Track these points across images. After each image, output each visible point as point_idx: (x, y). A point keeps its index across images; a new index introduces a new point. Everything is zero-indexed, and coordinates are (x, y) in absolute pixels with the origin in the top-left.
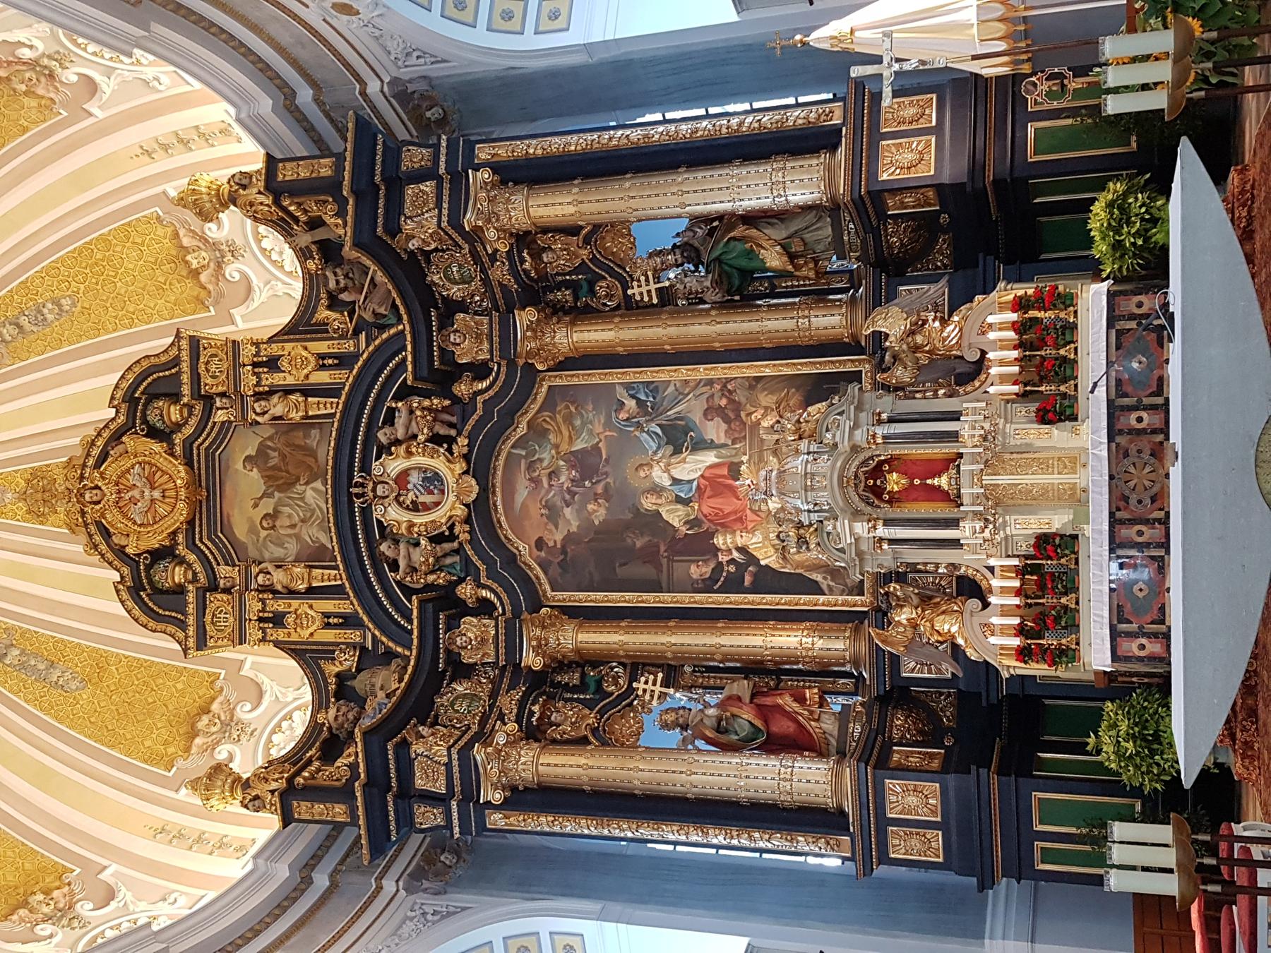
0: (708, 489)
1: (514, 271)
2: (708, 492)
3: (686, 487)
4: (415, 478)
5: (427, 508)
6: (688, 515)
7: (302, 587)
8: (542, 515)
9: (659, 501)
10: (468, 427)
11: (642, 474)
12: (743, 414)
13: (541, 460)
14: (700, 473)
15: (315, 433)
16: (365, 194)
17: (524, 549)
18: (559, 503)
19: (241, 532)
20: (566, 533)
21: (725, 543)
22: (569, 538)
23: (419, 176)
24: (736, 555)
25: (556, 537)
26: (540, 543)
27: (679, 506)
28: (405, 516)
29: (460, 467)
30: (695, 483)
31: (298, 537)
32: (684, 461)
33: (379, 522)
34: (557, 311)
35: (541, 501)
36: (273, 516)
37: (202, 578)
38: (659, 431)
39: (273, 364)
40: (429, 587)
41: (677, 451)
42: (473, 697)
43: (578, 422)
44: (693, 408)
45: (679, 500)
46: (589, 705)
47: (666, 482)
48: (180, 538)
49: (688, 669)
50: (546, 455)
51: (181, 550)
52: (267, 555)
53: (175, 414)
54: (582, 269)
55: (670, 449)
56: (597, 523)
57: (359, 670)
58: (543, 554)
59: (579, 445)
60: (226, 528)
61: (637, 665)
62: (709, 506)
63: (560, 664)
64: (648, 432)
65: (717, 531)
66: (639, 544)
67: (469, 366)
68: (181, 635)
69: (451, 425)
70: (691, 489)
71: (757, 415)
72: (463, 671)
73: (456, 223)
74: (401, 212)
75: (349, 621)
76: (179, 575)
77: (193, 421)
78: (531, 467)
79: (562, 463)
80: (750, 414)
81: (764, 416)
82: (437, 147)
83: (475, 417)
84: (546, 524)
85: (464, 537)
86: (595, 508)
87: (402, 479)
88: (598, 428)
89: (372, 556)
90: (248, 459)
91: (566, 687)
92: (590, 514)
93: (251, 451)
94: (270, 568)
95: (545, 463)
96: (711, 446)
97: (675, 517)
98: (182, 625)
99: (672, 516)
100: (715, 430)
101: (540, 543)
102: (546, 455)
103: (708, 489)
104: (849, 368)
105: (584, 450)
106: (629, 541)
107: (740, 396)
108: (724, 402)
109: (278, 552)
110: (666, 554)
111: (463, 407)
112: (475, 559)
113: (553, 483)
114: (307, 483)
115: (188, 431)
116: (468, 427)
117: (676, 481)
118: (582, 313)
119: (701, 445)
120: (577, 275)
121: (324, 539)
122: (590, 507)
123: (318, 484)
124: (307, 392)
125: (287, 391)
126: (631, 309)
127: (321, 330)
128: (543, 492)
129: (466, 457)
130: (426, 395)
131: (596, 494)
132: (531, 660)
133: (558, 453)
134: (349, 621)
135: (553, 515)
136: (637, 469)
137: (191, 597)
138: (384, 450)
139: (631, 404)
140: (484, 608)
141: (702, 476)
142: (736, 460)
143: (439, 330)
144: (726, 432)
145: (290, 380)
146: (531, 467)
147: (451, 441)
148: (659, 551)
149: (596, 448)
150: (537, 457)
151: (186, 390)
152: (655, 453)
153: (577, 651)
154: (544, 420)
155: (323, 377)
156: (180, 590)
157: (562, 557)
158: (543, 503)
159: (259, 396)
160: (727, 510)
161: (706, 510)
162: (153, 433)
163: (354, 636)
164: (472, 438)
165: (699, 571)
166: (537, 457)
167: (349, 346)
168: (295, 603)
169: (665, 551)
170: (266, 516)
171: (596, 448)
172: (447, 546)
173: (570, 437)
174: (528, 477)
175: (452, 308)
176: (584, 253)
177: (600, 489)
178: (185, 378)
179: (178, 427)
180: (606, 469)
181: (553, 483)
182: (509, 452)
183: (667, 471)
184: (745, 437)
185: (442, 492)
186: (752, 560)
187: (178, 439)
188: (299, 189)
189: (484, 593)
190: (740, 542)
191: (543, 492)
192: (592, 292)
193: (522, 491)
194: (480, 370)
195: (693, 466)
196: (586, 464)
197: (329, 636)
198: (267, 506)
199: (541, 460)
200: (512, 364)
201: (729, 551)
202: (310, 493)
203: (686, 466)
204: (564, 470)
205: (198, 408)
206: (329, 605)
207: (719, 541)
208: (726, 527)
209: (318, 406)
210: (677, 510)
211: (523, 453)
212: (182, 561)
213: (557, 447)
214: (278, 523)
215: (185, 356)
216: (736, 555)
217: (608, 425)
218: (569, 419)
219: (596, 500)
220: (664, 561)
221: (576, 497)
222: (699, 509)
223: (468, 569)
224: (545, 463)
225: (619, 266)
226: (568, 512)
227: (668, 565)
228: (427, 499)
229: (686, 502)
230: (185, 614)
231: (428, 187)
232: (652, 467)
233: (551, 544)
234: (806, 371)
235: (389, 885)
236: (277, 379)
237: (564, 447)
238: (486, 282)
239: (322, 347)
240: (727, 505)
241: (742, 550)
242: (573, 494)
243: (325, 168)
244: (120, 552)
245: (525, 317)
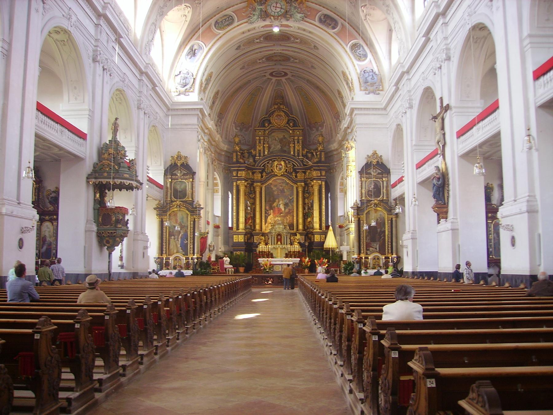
1: (309, 183)
4: (281, 166)
5: (276, 168)
7: (265, 145)
10: (288, 174)
15: (288, 147)
16: (318, 166)
17: (270, 182)
19: (273, 134)
22: (272, 188)
23: (321, 173)
24: (270, 213)
25: (272, 187)
28: (275, 165)
29: (282, 173)
31: (272, 144)
33: (274, 161)
34: (304, 188)
36: (276, 140)
37: (266, 129)
39: (298, 142)
40: (265, 168)
41: (284, 205)
42: (249, 176)
43: (289, 190)
44: (290, 207)
45: (277, 205)
46: (248, 193)
47: (280, 203)
48: (272, 125)
49: (254, 206)
50: (284, 185)
51: (270, 125)
52: (270, 138)
53: (291, 124)
54: (310, 192)
57: (252, 156)
59: (285, 190)
60: (274, 132)
61: (254, 199)
62: (276, 210)
63: (254, 188)
66: (272, 199)
67: (297, 175)
68: (257, 126)
69: (288, 172)
71: (289, 216)
72: (253, 173)
73: (314, 179)
74: (316, 171)
75: (260, 154)
76: (266, 125)
77: (290, 128)
82: (325, 176)
83: (289, 175)
85: (272, 174)
87: (281, 165)
88: (288, 193)
89: (269, 159)
90: (284, 136)
91: (251, 188)
93: (286, 136)
94: (268, 140)
96: (285, 210)
97: (275, 204)
98: (258, 127)
100: (287, 210)
101: (271, 184)
102: (284, 185)
104: (295, 229)
107: (291, 214)
108: (291, 212)
109: (270, 141)
111: (291, 174)
112: (269, 175)
114: (281, 146)
115: (289, 126)
116: (288, 174)
117: (280, 204)
118: (304, 192)
119: (285, 208)
121: (272, 148)
122: (277, 192)
123: (280, 148)
124: (294, 147)
125: (294, 144)
126: (304, 199)
127: (303, 150)
129: (284, 174)
130: (293, 168)
132: (255, 184)
134: (260, 154)
135: (275, 186)
137: (263, 128)
138: (285, 163)
139: (291, 198)
140: (262, 177)
143: (302, 171)
145: (296, 145)
146: (282, 183)
147: (286, 172)
149: (285, 193)
151: (295, 128)
153: (256, 191)
155: (296, 150)
156: (264, 126)
159: (294, 139)
162: (288, 120)
163: (258, 155)
164: (287, 175)
165: (267, 207)
167: (301, 154)
168: (262, 145)
170: (275, 139)
171: (285, 193)
172: (271, 171)
175: (305, 173)
176: (311, 193)
177: (279, 193)
178: (297, 128)
179: (289, 125)
185: (279, 171)
186: (269, 215)
187: (288, 125)
188: (320, 155)
189: (264, 177)
190: (272, 214)
192: (307, 193)
193: (279, 181)
194: (296, 176)
195: (282, 207)
196: (283, 191)
197: (257, 150)
198: (277, 139)
200: (297, 181)
202: (279, 146)
205: (292, 129)
206: (262, 150)
207: (272, 211)
208: (273, 212)
209: (292, 149)
212: (269, 125)
213: (285, 187)
214: (274, 141)
215: (300, 128)
216: (270, 213)
217: (288, 195)
218: (289, 188)
223: (267, 174)
226: (276, 188)
228: (278, 168)
229: (277, 206)
230: (261, 127)
231: (319, 175)
234: (295, 223)
235: (223, 164)
236: (296, 142)
237: (285, 188)
238: (308, 178)
239: (301, 150)
240: (277, 212)
241: (270, 214)
243: (323, 159)
244: (270, 116)
245: (303, 184)
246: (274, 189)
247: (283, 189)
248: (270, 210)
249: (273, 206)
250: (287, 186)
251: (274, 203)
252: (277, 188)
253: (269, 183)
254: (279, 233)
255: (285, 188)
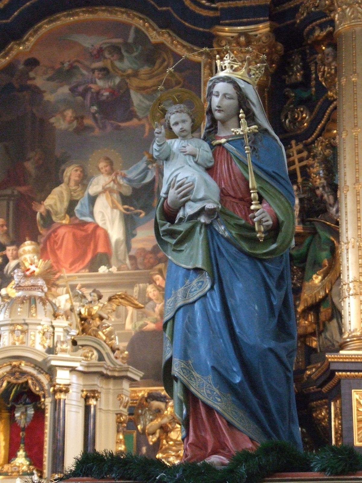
0: (83, 233)
2: (80, 233)
3: (86, 210)
6: (56, 213)
8: (62, 63)
9: (72, 183)
11: (102, 165)
12: (161, 266)
13: (121, 59)
14: (100, 223)
18: (75, 80)
20: (43, 89)
21: (25, 252)
22: (37, 92)
26: (32, 63)
27: (66, 204)
30: (89, 219)
32: (114, 207)
35: (78, 61)
38: (148, 179)
41: (125, 200)
45: (73, 203)
55: (127, 191)
56: (52, 120)
58: (21, 67)
59: (136, 98)
64: (146, 170)
65: (38, 244)
66: (30, 166)
70: (85, 216)
71: (159, 280)
78: (115, 49)
79: (117, 80)
80: (161, 272)
81: (159, 288)
84: (53, 68)
86: (68, 118)
92: (62, 113)
95: (118, 64)
99: (56, 197)
101: (32, 63)
103: (83, 233)
105: (128, 102)
106: (31, 154)
110: (16, 193)
113: (96, 72)
117: (92, 200)
120: (315, 86)
122: (69, 114)
128: (87, 63)
131: (82, 118)
133: (129, 76)
136: (107, 159)
141: (97, 227)
142: (113, 260)
144: (143, 250)
146: (115, 49)
148: (20, 185)
149: (132, 115)
150: (125, 54)
152: (124, 177)
154: (164, 60)
157: (17, 86)
158: (76, 64)
160: (61, 254)
161: (61, 232)
166: (125, 54)
169: (19, 192)
171: (132, 115)
173: (144, 88)
174: (105, 46)
177: (89, 122)
180: (109, 128)
181: (96, 72)
182: (126, 27)
183: (105, 190)
184: (138, 269)
191: (87, 63)
199: (121, 59)
201: (16, 257)
203: (109, 209)
204: (110, 84)
207: (28, 246)
210: (61, 201)
211: (130, 40)
213: (135, 74)
219: (76, 118)
220: (9, 192)
221: (80, 98)
222: (62, 225)
224: (118, 64)
225: (323, 129)
226: (65, 90)
227: (5, 196)
229: (70, 210)
232: (109, 174)
233: (32, 74)
237: (134, 82)
242: (83, 94)
246: (49, 97)
247: (113, 92)
248: (18, 242)
249: (41, 210)
250: (145, 70)
251: (49, 193)
252: (72, 90)
253: (14, 53)
254: (16, 371)
255: (134, 82)
